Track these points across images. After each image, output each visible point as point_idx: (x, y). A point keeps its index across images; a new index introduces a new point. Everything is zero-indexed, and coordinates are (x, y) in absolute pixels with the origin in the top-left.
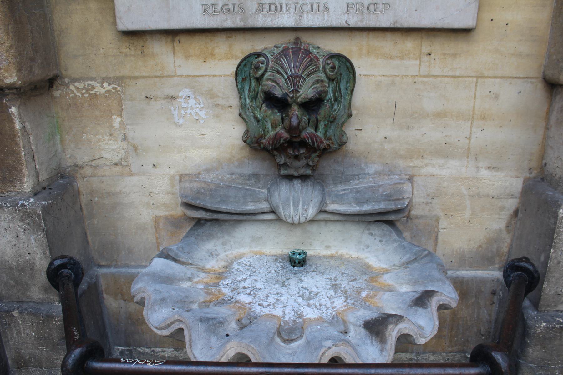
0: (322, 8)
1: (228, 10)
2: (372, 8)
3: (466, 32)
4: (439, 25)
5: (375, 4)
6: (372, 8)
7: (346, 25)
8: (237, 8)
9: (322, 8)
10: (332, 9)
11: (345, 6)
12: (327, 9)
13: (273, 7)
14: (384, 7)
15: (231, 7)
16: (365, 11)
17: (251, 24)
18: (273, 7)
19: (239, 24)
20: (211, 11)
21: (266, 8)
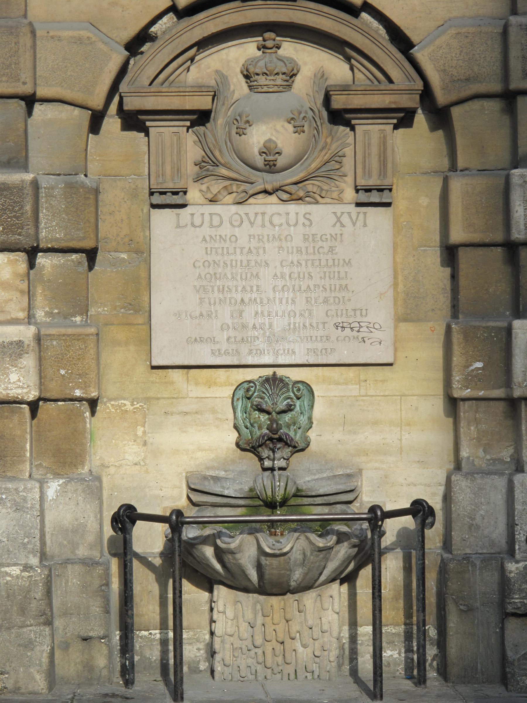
0: (290, 352)
1: (228, 353)
2: (324, 351)
3: (391, 365)
4: (369, 361)
5: (326, 349)
6: (324, 351)
7: (307, 363)
8: (234, 351)
9: (290, 352)
10: (297, 353)
11: (306, 350)
12: (294, 353)
13: (259, 352)
14: (331, 351)
15: (230, 351)
16: (319, 353)
17: (243, 363)
18: (259, 352)
19: (236, 363)
20: (217, 354)
21: (254, 352)
